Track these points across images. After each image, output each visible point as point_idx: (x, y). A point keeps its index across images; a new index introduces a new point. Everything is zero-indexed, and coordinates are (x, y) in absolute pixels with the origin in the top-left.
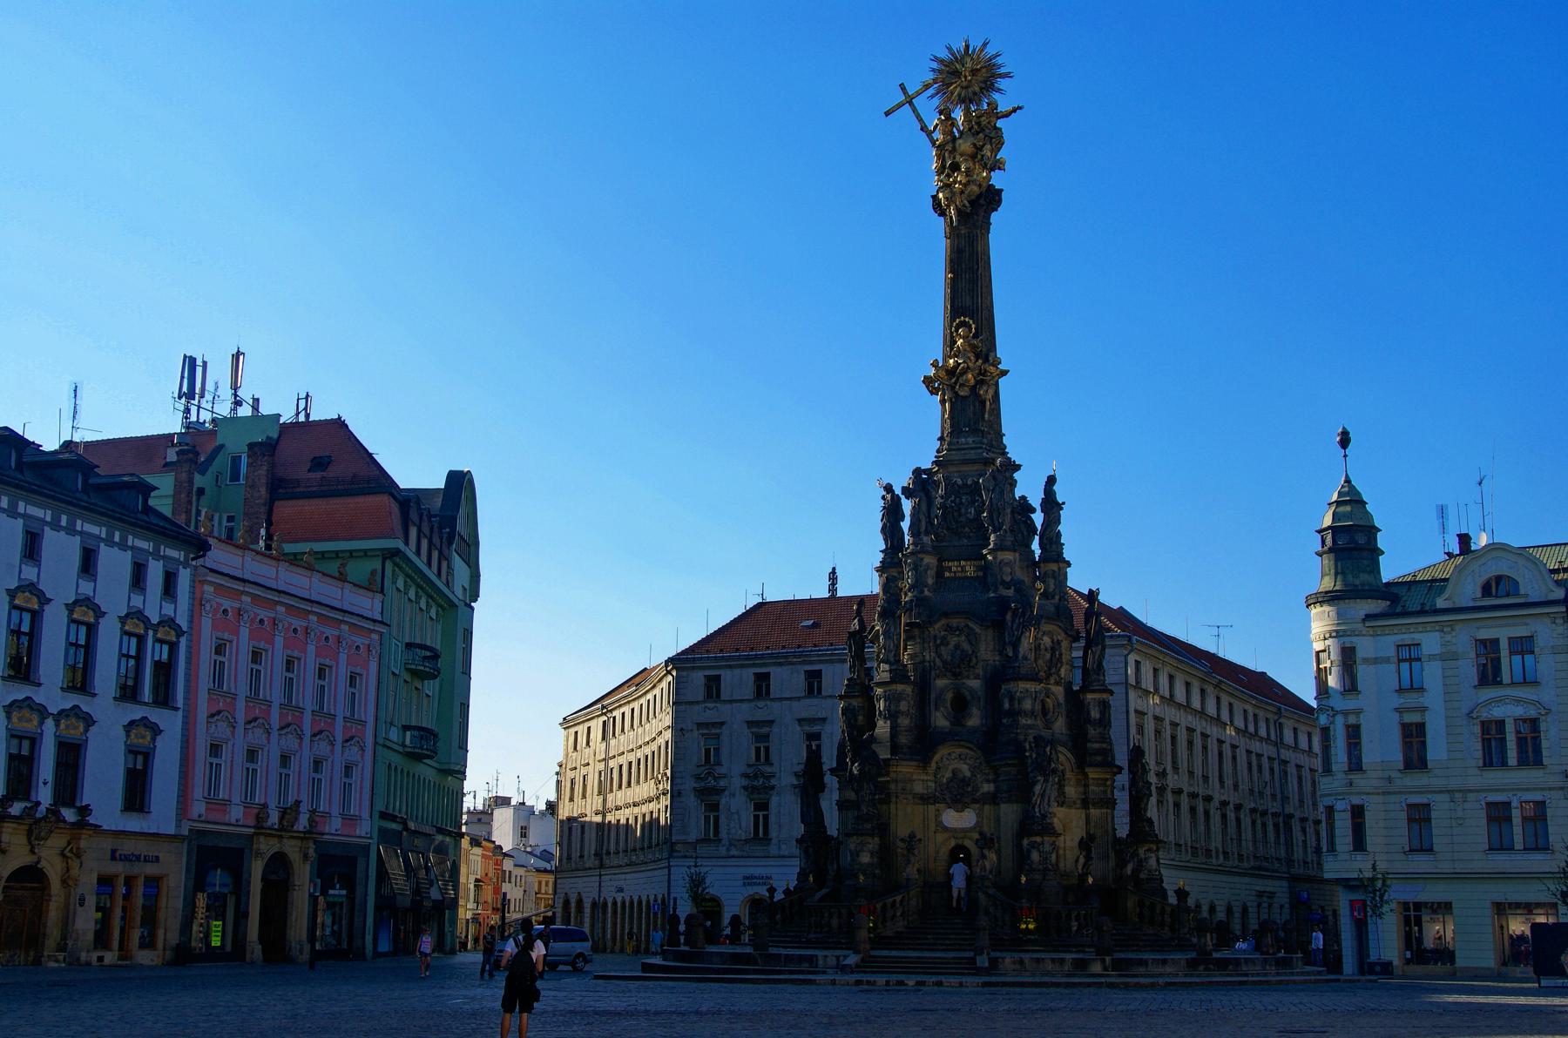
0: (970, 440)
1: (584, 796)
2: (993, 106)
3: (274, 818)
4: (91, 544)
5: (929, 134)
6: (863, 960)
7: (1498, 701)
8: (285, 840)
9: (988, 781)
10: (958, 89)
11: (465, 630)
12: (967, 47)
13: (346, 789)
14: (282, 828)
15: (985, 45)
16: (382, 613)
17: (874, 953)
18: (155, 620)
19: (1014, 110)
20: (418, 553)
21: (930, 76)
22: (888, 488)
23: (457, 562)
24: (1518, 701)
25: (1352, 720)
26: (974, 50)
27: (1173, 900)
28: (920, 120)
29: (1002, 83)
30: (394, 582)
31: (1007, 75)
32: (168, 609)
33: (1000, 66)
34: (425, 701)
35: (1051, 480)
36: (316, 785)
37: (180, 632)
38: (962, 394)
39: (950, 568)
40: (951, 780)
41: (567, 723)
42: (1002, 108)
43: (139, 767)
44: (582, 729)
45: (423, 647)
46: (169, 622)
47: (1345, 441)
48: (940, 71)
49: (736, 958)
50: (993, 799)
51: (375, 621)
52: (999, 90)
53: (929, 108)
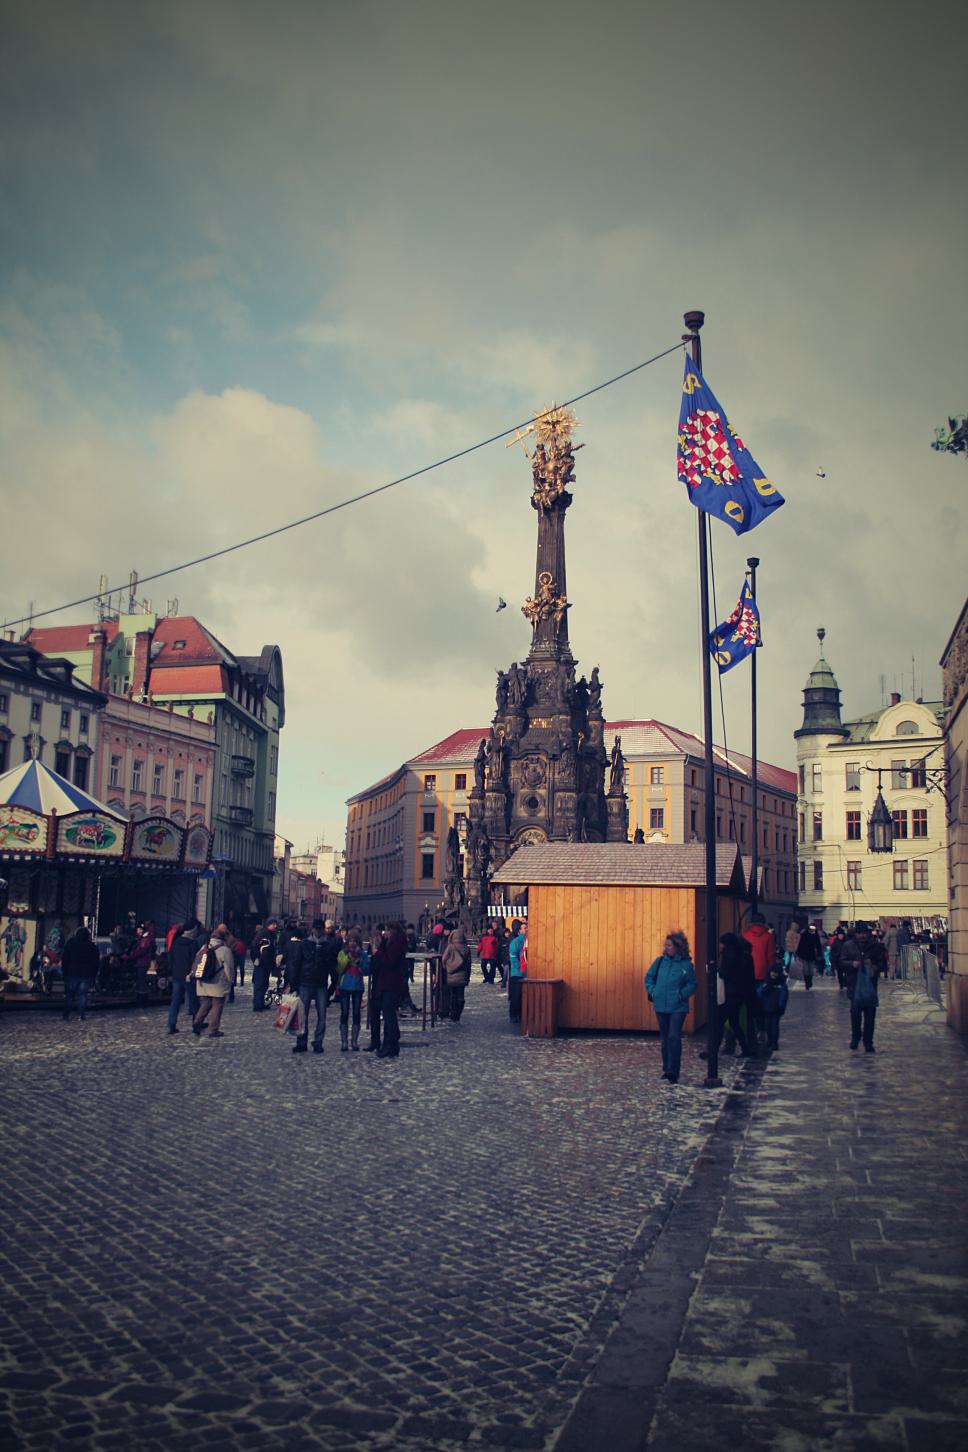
4: (37, 701)
7: (901, 799)
11: (273, 747)
18: (75, 745)
20: (240, 701)
23: (269, 704)
30: (224, 719)
32: (83, 739)
34: (246, 792)
35: (596, 671)
37: (90, 752)
46: (84, 747)
47: (821, 635)
51: (210, 743)
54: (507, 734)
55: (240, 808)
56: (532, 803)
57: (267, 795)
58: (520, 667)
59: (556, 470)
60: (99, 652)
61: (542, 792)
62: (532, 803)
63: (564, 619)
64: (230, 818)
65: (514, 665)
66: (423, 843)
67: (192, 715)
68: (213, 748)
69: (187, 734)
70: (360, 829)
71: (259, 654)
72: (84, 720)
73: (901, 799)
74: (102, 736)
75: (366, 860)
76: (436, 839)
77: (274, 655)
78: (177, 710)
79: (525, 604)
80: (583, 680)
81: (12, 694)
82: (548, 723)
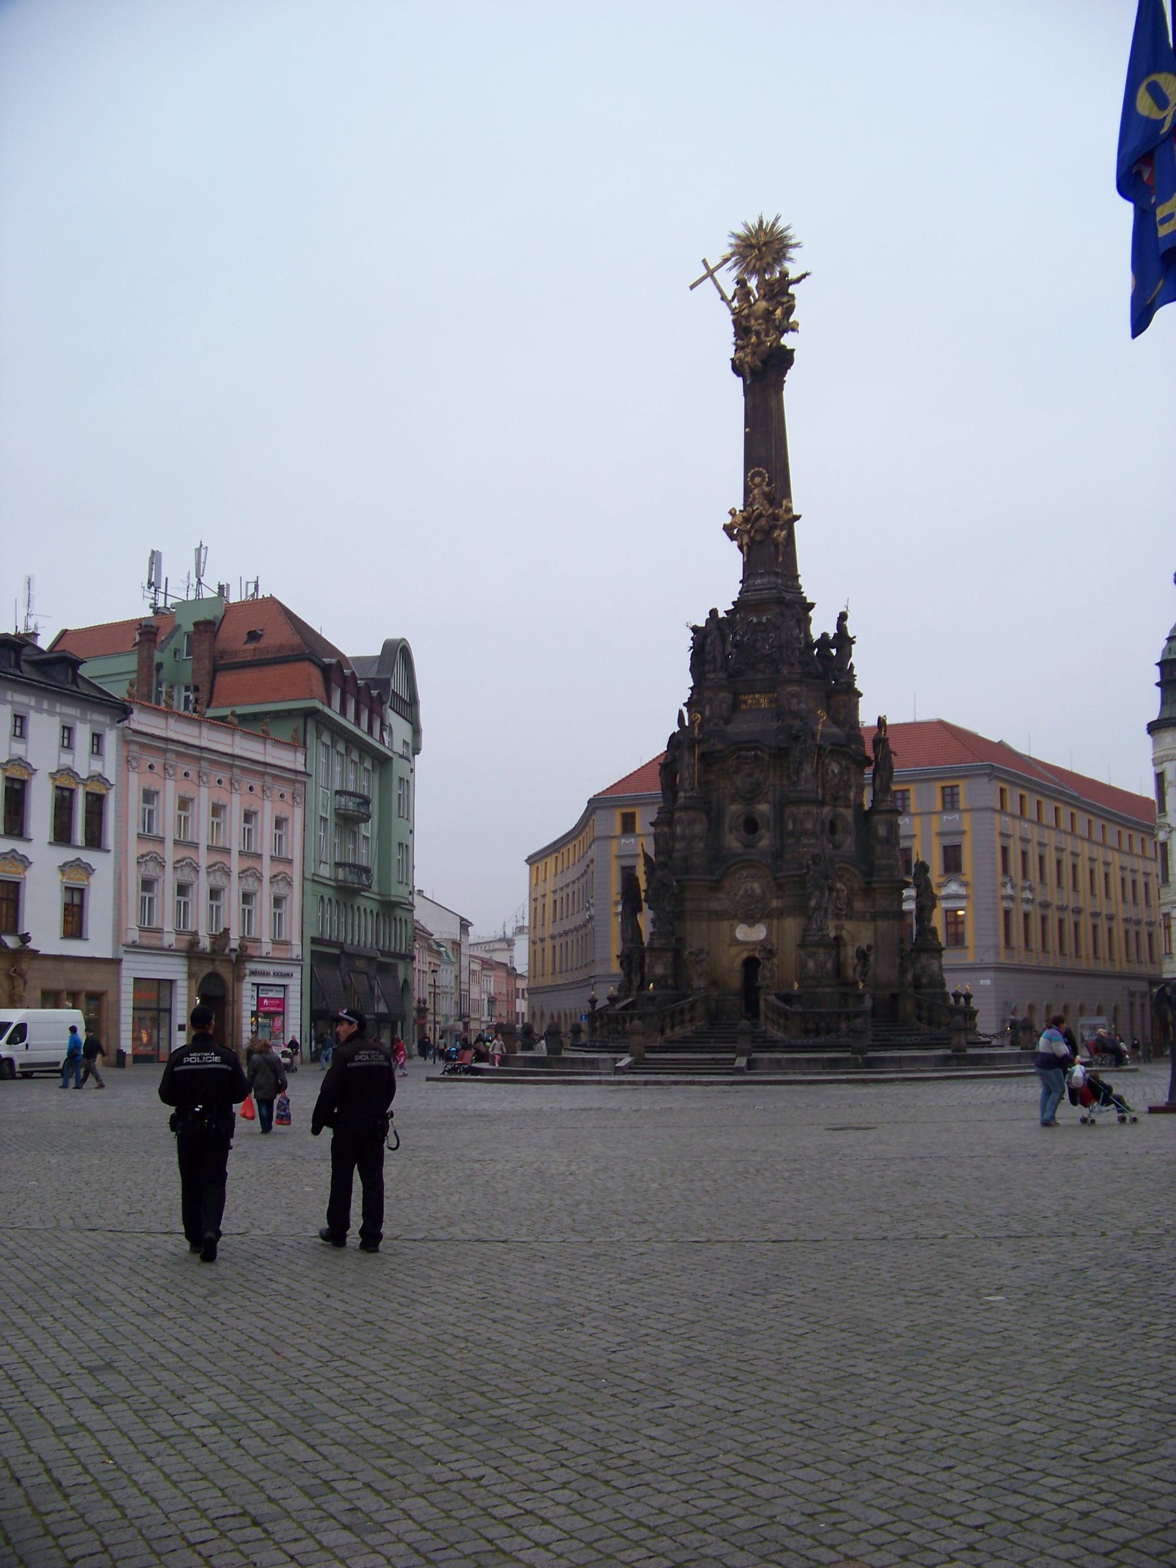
0: (766, 580)
1: (543, 925)
2: (784, 275)
3: (205, 943)
5: (729, 303)
6: (636, 1062)
8: (217, 963)
9: (777, 898)
10: (754, 261)
12: (761, 223)
13: (278, 919)
14: (213, 951)
15: (777, 219)
16: (305, 765)
17: (648, 1055)
18: (84, 775)
19: (804, 276)
20: (343, 711)
21: (729, 251)
23: (393, 718)
26: (767, 225)
28: (720, 291)
29: (792, 253)
31: (796, 246)
32: (97, 767)
33: (791, 238)
35: (843, 617)
36: (247, 916)
38: (758, 538)
39: (745, 702)
41: (532, 860)
42: (792, 276)
43: (76, 901)
44: (541, 865)
46: (99, 778)
48: (737, 246)
49: (535, 1061)
50: (781, 913)
51: (296, 772)
52: (790, 259)
53: (728, 279)
56: (751, 825)
57: (395, 848)
58: (721, 615)
61: (764, 808)
62: (751, 825)
64: (336, 880)
65: (713, 612)
68: (300, 778)
69: (229, 750)
70: (544, 896)
71: (379, 654)
72: (97, 739)
74: (127, 762)
75: (553, 937)
79: (728, 520)
80: (824, 635)
81: (32, 712)
82: (771, 701)
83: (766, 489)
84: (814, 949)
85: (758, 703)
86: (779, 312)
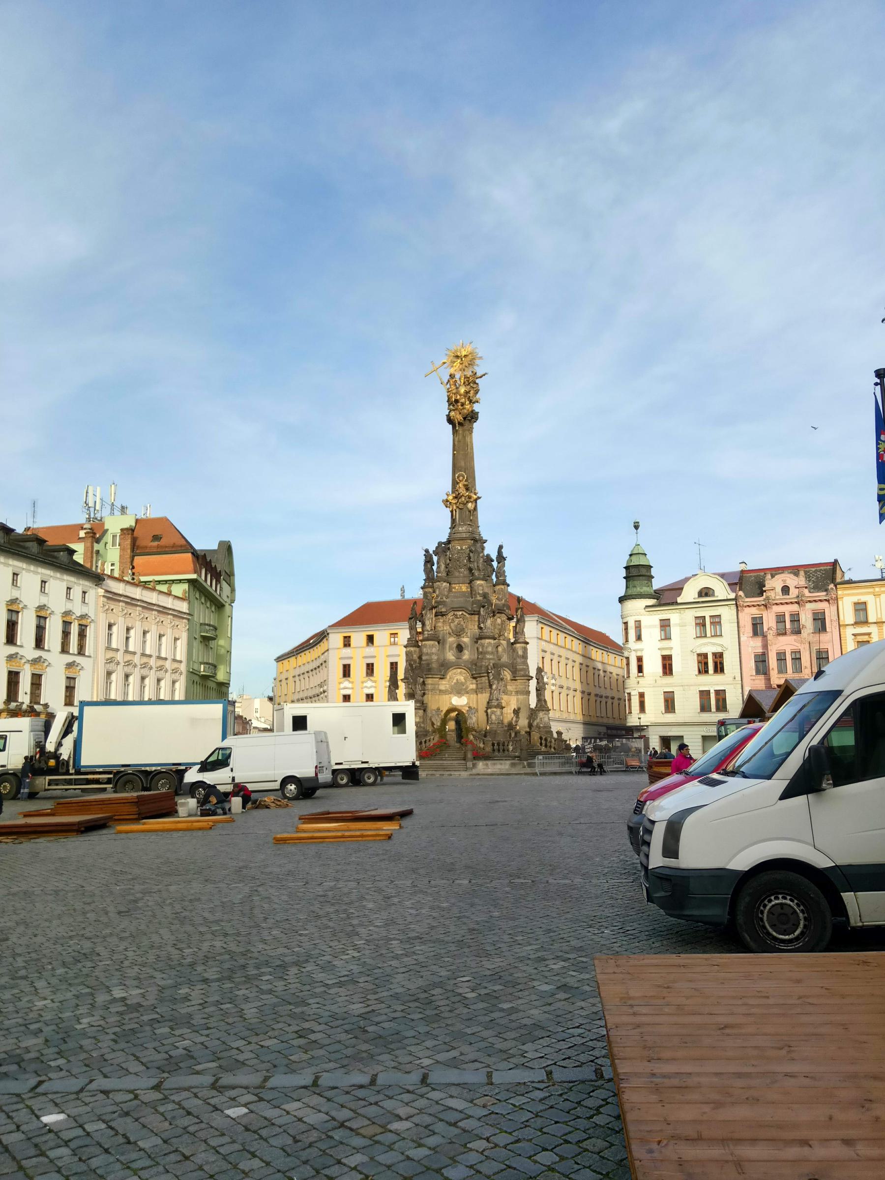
7: (705, 644)
22: (427, 551)
23: (224, 584)
24: (714, 644)
25: (639, 654)
27: (555, 735)
31: (481, 358)
35: (501, 547)
39: (455, 588)
40: (455, 684)
41: (279, 659)
42: (479, 374)
45: (209, 625)
47: (636, 527)
54: (437, 596)
55: (207, 663)
56: (460, 648)
59: (467, 393)
60: (89, 544)
62: (460, 648)
63: (475, 509)
66: (342, 686)
67: (171, 592)
73: (705, 644)
76: (352, 683)
77: (227, 548)
78: (159, 587)
79: (445, 497)
83: (466, 483)
84: (495, 709)
85: (461, 589)
86: (472, 392)
